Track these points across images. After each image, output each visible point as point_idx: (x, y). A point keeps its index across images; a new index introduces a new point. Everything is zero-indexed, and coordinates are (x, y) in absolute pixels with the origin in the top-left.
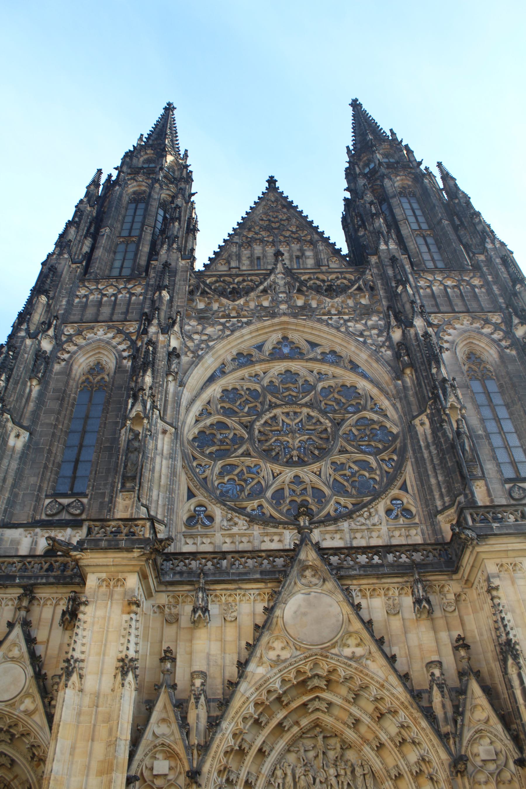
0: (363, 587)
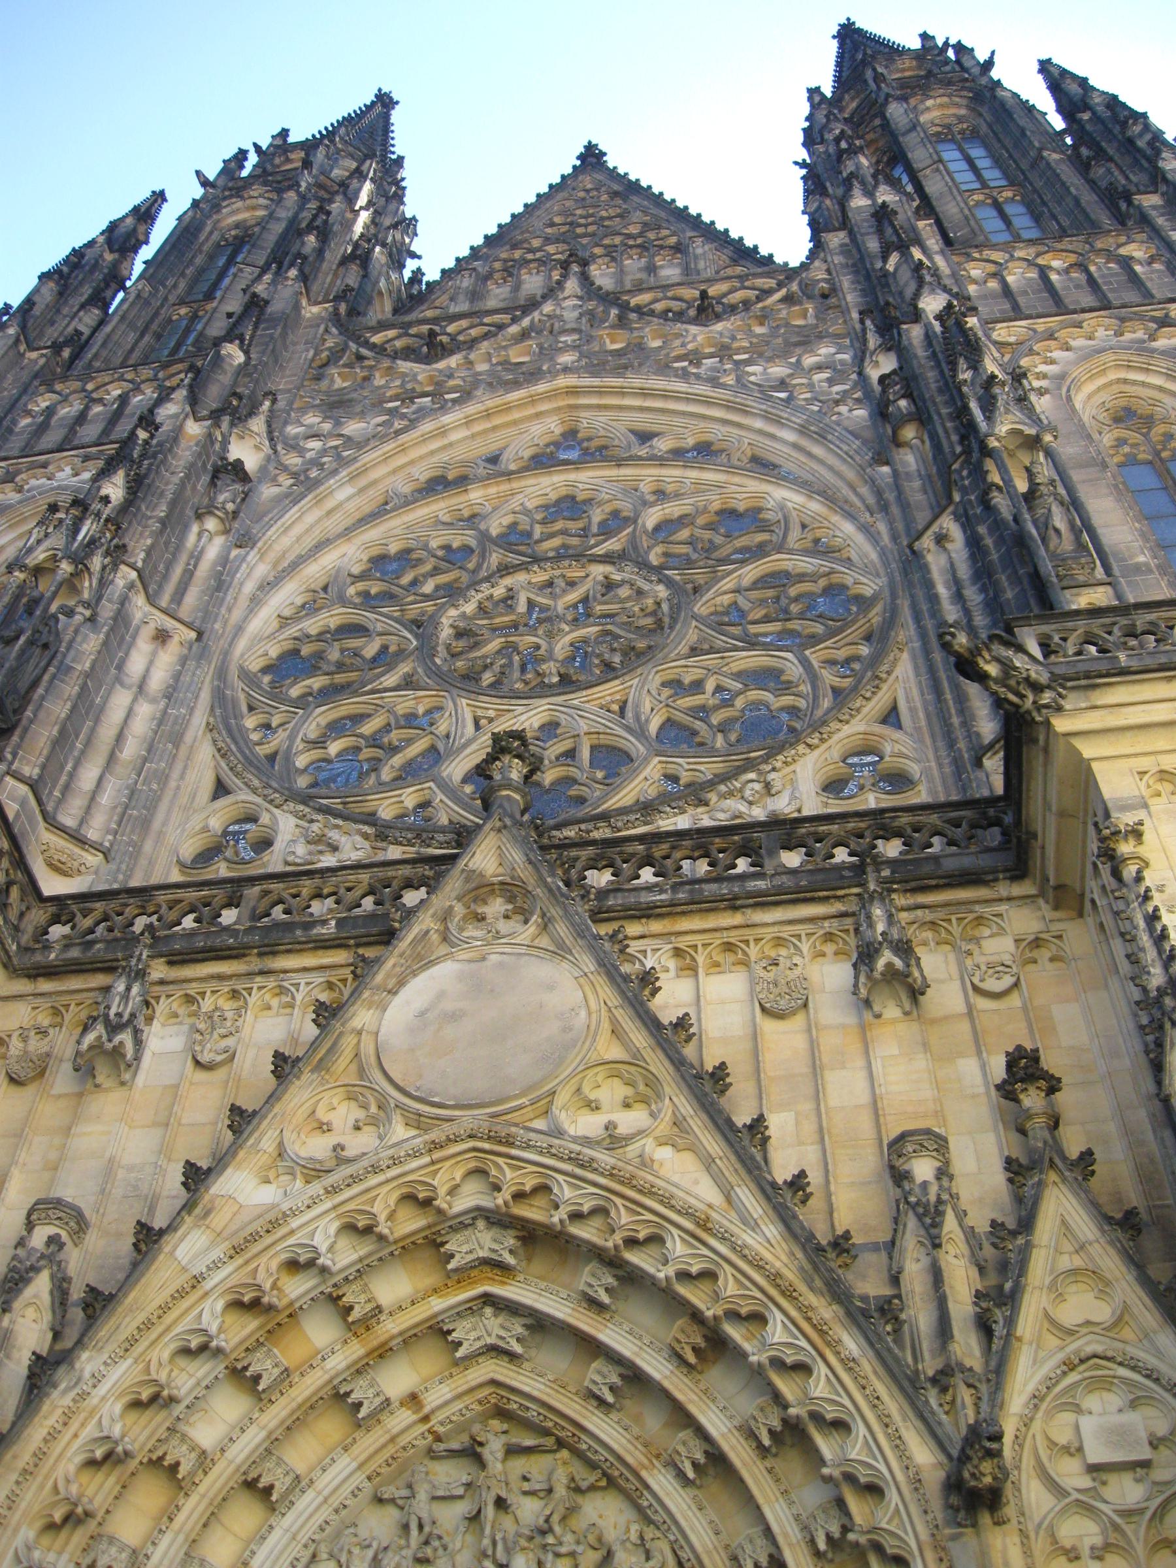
0: (683, 942)
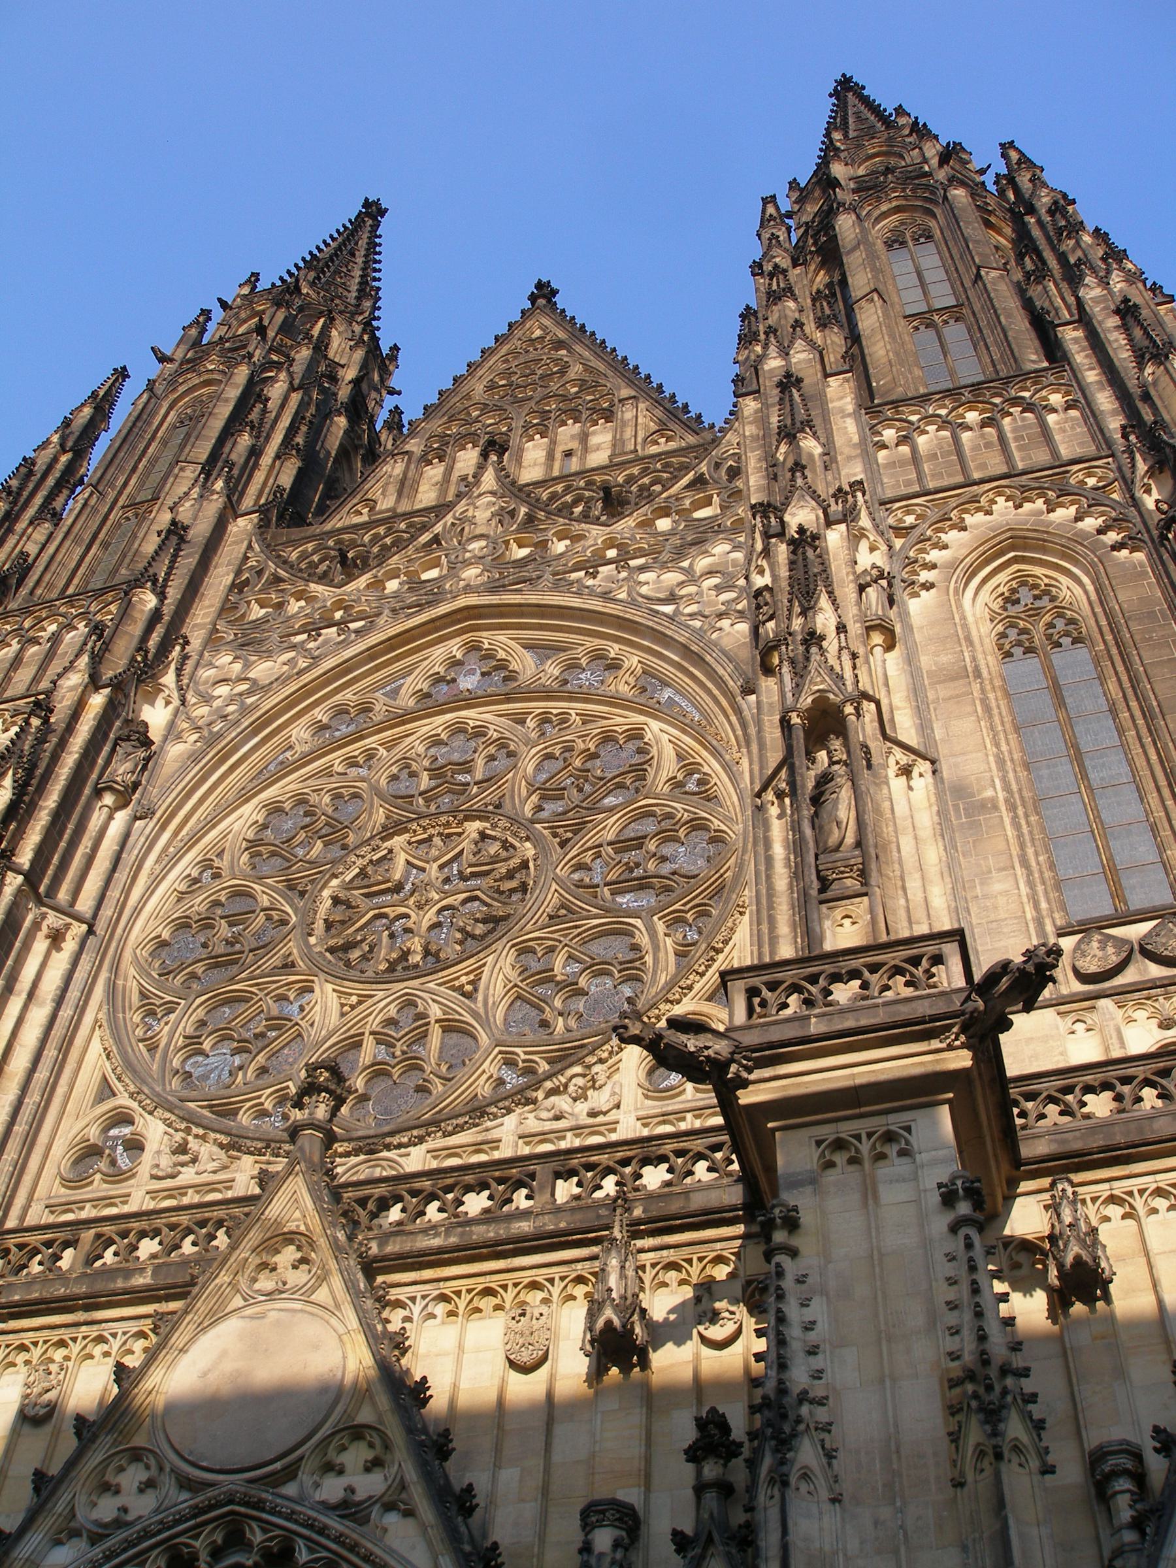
0: (447, 1288)
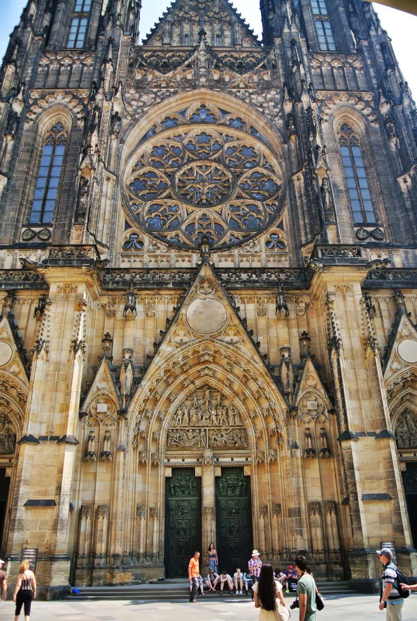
0: (243, 296)
